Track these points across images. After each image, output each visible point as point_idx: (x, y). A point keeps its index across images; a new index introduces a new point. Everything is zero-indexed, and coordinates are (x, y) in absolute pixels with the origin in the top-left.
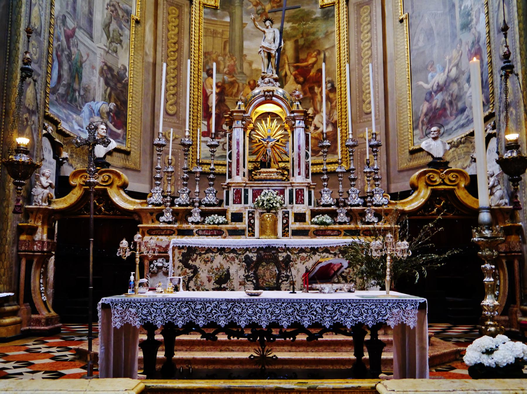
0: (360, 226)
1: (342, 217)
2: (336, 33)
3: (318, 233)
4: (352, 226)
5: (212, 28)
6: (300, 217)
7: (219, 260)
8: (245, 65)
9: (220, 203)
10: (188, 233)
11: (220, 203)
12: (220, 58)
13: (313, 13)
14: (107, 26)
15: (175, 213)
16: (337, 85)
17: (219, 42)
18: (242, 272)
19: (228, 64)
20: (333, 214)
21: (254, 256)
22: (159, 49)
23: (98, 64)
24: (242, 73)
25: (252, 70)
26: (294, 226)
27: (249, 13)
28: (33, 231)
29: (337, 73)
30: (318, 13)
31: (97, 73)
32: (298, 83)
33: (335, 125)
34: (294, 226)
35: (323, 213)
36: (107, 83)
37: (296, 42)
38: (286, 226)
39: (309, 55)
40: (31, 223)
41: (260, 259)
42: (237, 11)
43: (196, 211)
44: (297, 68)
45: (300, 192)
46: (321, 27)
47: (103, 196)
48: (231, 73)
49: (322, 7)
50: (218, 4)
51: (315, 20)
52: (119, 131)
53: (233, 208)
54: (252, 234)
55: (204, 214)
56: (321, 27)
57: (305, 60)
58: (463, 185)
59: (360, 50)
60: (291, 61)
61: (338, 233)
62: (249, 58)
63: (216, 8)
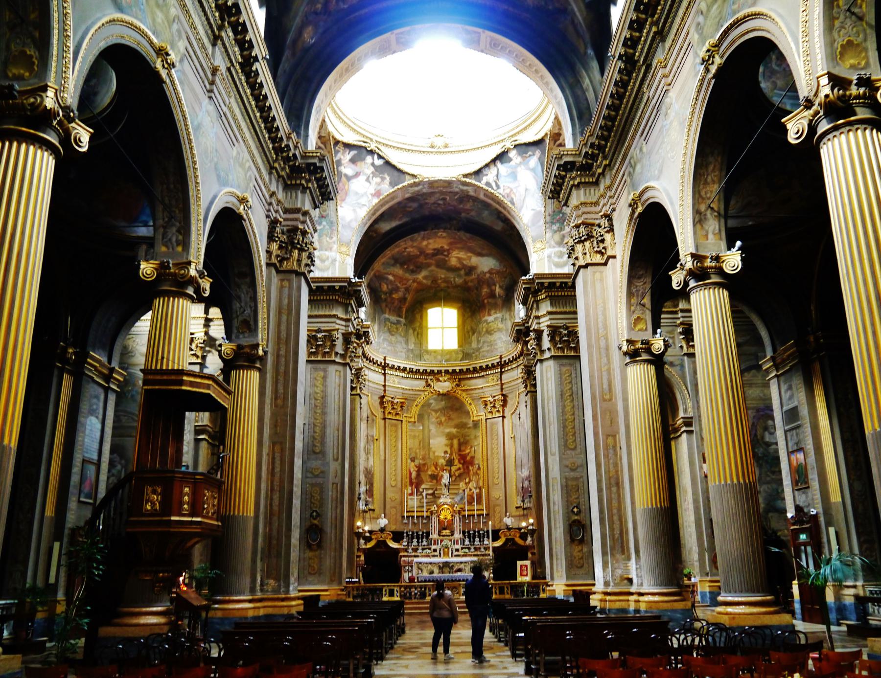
0: (479, 553)
1: (472, 550)
2: (481, 436)
3: (463, 556)
4: (476, 553)
5: (413, 434)
6: (457, 550)
7: (430, 566)
8: (431, 454)
9: (428, 545)
10: (418, 556)
11: (428, 545)
12: (418, 451)
13: (468, 424)
14: (365, 448)
15: (412, 549)
16: (481, 466)
17: (417, 442)
18: (438, 571)
19: (422, 453)
20: (469, 549)
21: (441, 565)
22: (387, 451)
23: (362, 468)
24: (429, 458)
25: (435, 457)
26: (455, 553)
27: (432, 423)
28: (359, 557)
29: (481, 460)
30: (471, 425)
31: (362, 473)
32: (460, 463)
33: (480, 489)
34: (455, 553)
35: (465, 548)
36: (366, 477)
37: (459, 440)
38: (452, 554)
39: (466, 448)
40: (359, 554)
41: (443, 566)
42: (426, 422)
43: (420, 548)
44: (460, 455)
45: (457, 541)
46: (473, 432)
47: (384, 542)
48: (423, 459)
49: (473, 421)
50: (416, 420)
51: (469, 428)
52: (370, 500)
53: (433, 547)
54: (440, 556)
55: (423, 549)
56: (473, 432)
57: (464, 451)
58: (518, 535)
59: (492, 449)
60: (457, 451)
61: (471, 555)
62: (433, 449)
63: (415, 422)
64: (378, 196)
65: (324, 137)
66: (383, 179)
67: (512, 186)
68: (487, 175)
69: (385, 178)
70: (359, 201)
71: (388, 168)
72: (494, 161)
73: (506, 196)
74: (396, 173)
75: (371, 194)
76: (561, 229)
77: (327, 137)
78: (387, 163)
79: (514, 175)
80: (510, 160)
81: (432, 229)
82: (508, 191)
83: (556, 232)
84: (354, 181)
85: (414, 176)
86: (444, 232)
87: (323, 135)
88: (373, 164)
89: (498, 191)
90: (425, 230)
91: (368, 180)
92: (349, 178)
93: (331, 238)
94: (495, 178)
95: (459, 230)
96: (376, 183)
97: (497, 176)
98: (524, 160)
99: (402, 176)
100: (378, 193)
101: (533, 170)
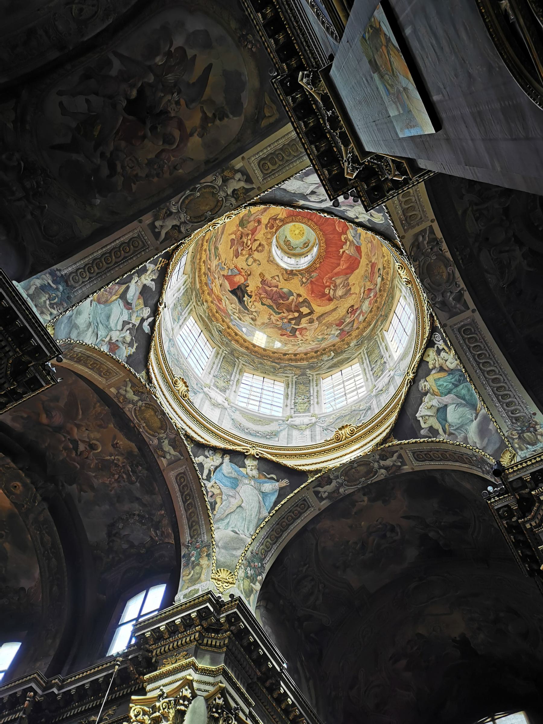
64: (111, 350)
65: (180, 232)
66: (131, 345)
67: (224, 489)
68: (207, 457)
69: (132, 347)
70: (100, 325)
71: (144, 342)
72: (225, 452)
73: (210, 494)
74: (141, 356)
75: (111, 339)
76: (253, 580)
77: (181, 237)
78: (150, 338)
79: (235, 483)
80: (244, 466)
81: (21, 469)
82: (216, 491)
83: (247, 577)
84: (122, 304)
85: (150, 380)
86: (25, 485)
87: (183, 229)
88: (143, 320)
89: (206, 482)
90: (14, 461)
91: (125, 323)
92: (123, 297)
93: (52, 306)
94: (212, 467)
95: (45, 499)
96: (124, 338)
97: (216, 468)
98: (259, 478)
99: (142, 366)
100: (114, 346)
101: (264, 495)
